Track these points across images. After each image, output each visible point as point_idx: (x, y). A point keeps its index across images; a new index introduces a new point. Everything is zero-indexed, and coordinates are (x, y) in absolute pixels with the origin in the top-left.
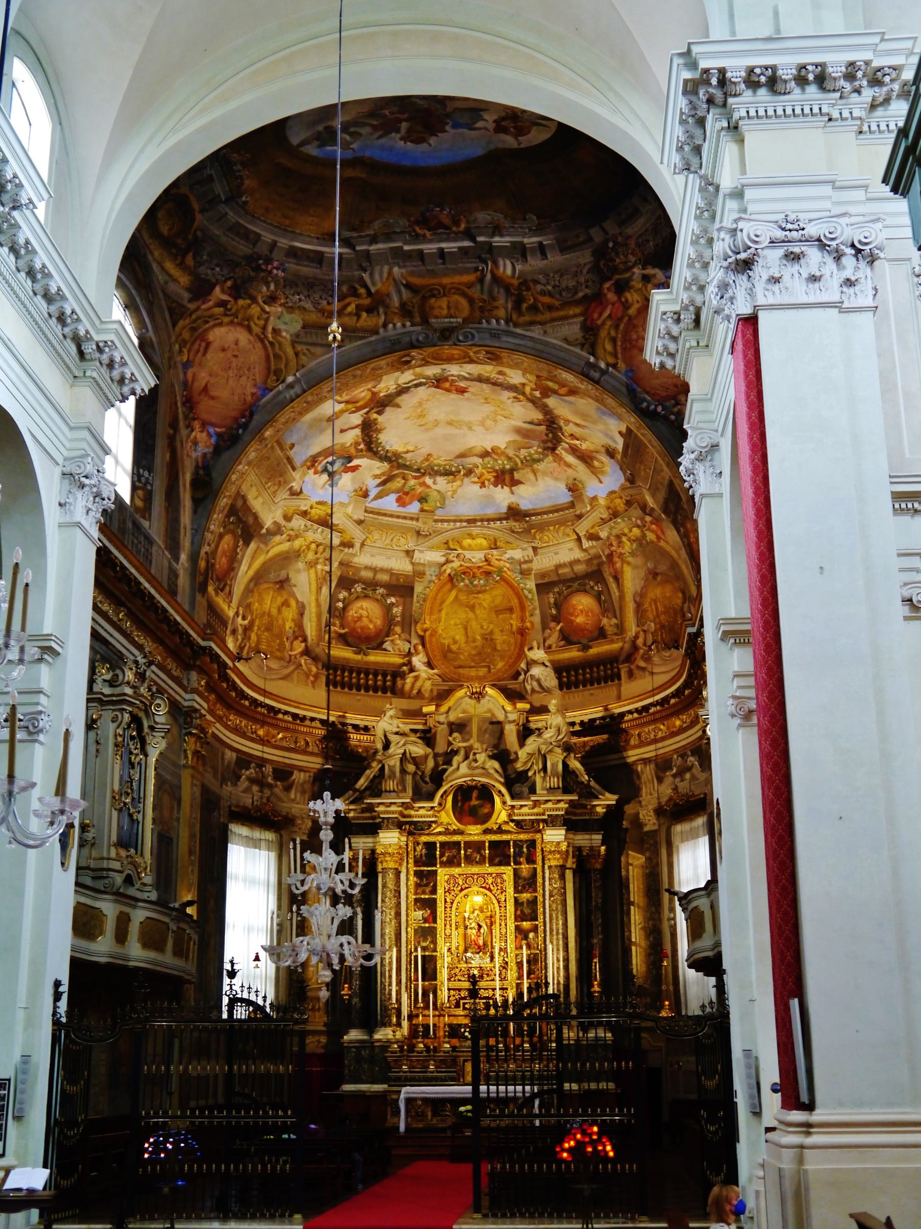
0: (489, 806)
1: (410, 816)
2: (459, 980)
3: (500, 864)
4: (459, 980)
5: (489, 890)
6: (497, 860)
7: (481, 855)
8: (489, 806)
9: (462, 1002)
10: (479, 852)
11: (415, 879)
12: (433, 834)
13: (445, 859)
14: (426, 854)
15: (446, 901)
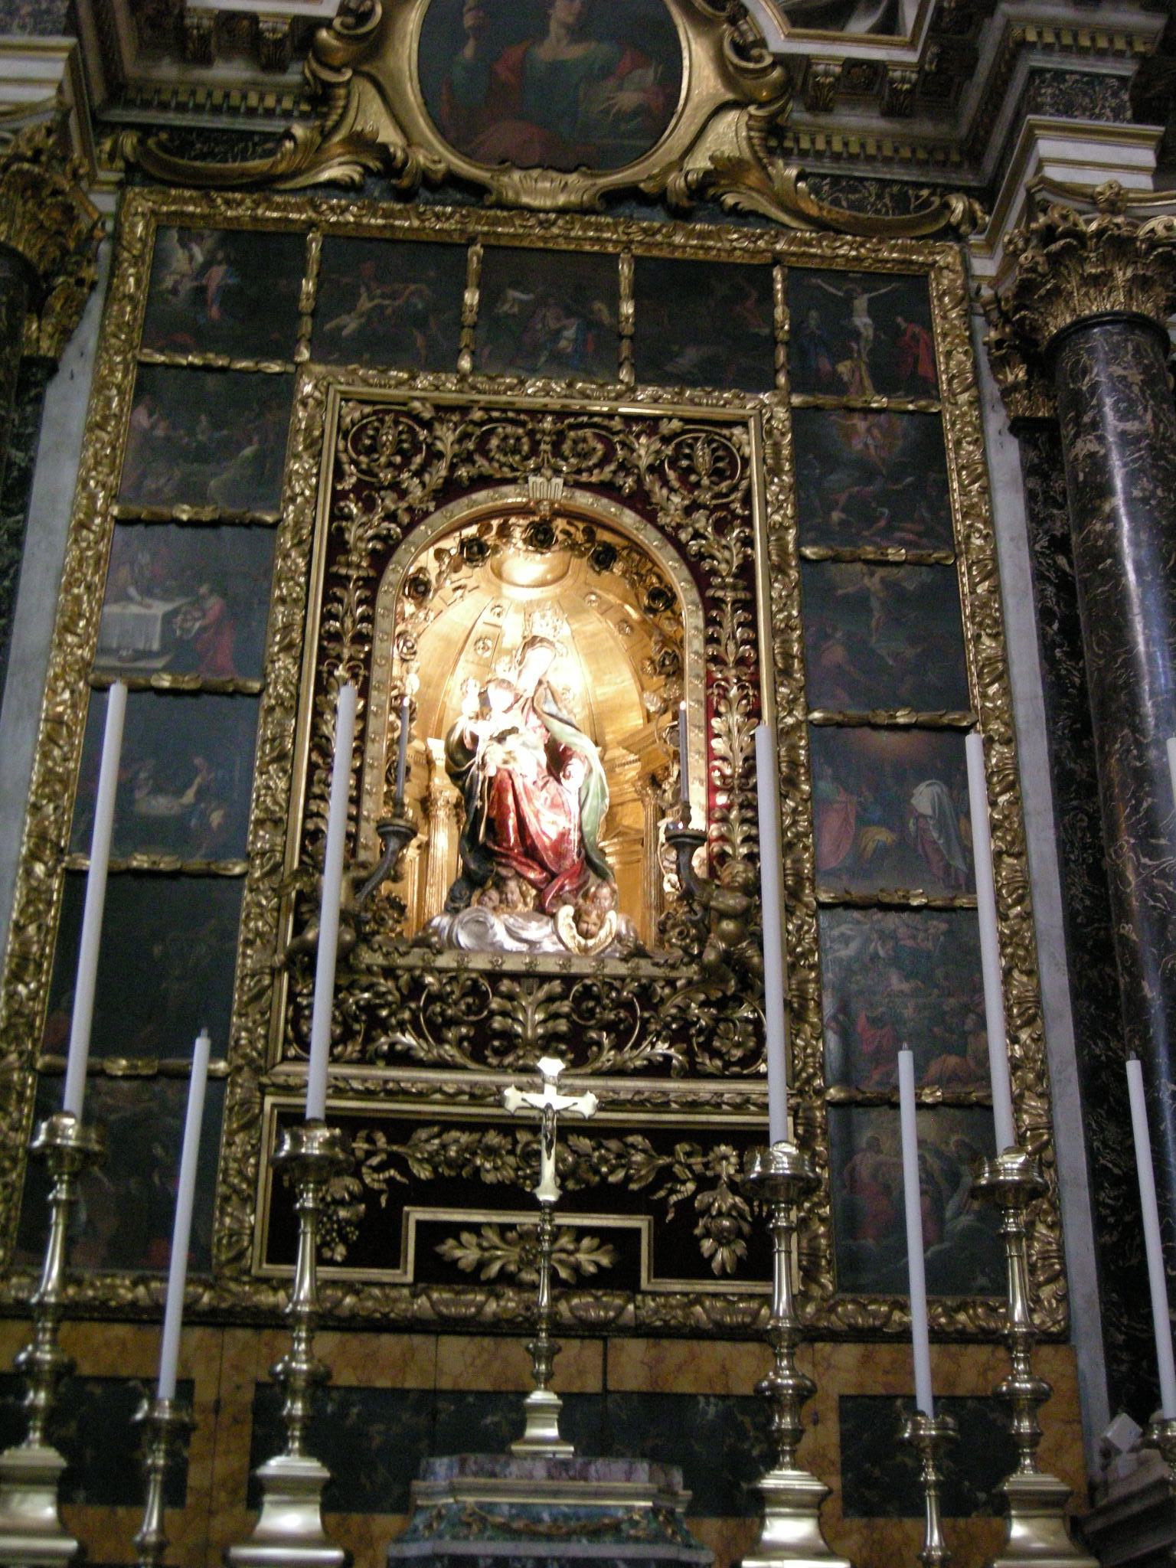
0: (649, 75)
1: (151, 97)
2: (401, 1058)
3: (711, 376)
4: (401, 1058)
5: (641, 502)
6: (690, 357)
7: (590, 324)
8: (649, 75)
9: (417, 1214)
10: (576, 305)
11: (142, 418)
12: (293, 191)
13: (350, 324)
14: (227, 295)
15: (337, 545)
